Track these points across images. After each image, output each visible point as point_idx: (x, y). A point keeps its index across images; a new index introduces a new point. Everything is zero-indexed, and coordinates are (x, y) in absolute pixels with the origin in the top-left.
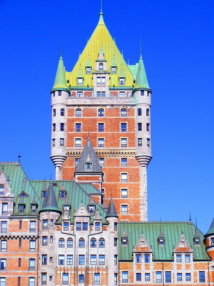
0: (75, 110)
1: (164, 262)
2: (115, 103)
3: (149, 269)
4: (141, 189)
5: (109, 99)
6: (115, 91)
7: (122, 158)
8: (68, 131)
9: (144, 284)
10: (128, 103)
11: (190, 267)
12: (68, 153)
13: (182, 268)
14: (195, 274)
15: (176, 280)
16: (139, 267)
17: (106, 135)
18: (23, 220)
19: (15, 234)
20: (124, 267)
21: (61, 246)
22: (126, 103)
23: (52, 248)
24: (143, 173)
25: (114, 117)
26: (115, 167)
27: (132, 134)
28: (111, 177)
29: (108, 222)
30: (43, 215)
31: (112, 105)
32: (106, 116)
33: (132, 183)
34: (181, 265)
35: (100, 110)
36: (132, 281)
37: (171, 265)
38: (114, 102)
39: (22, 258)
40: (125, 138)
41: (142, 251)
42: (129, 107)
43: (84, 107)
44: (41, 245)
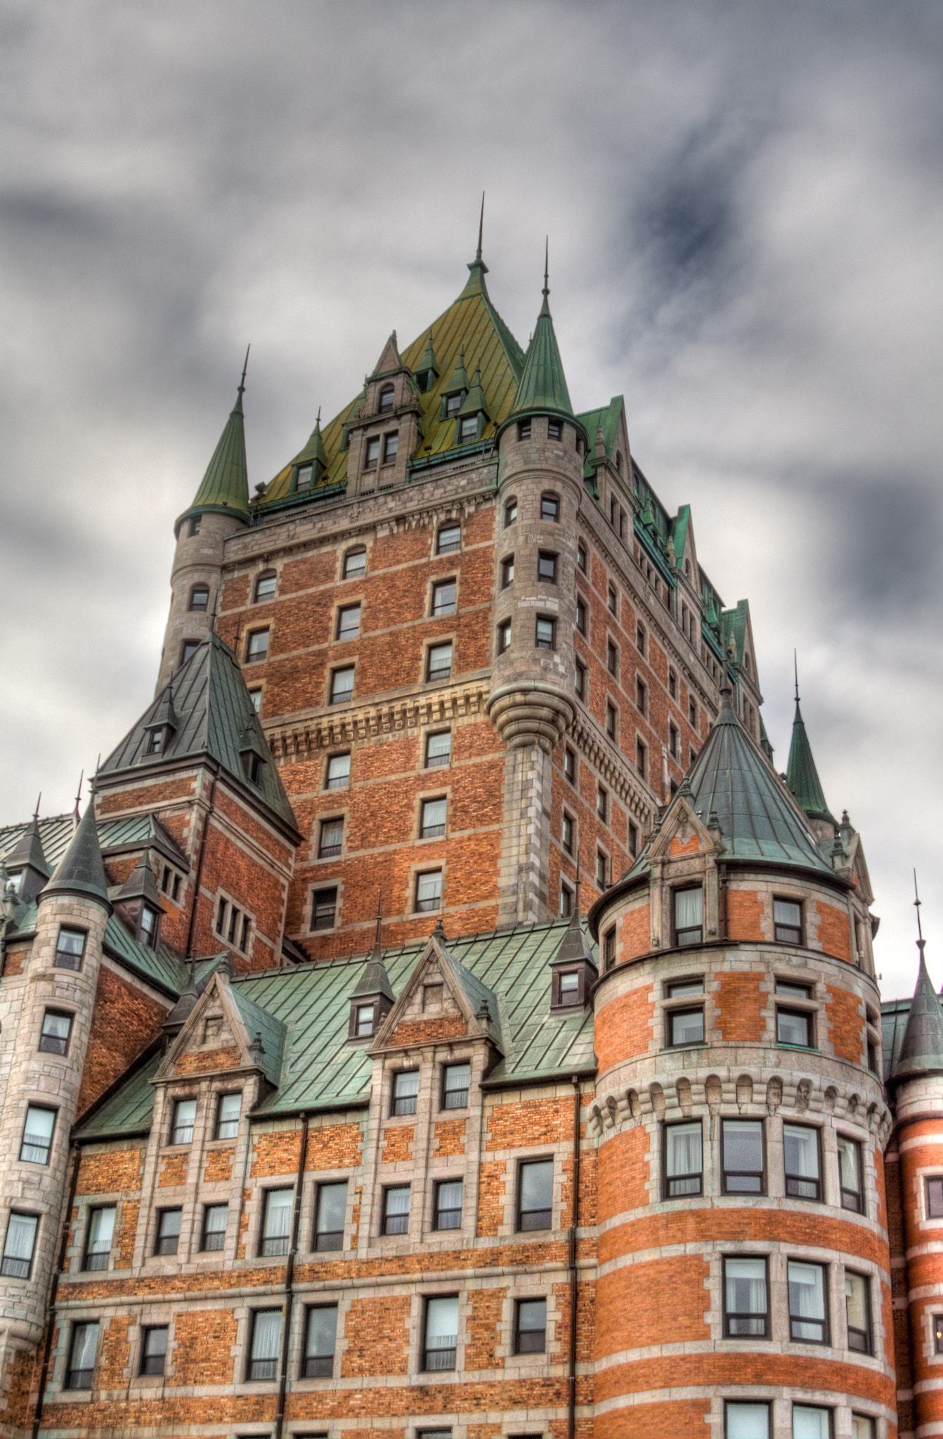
1: (314, 1123)
2: (412, 506)
3: (225, 1174)
4: (504, 854)
5: (389, 499)
6: (435, 471)
7: (424, 730)
9: (189, 1269)
10: (464, 491)
11: (464, 1139)
14: (487, 1178)
17: (362, 647)
20: (100, 1179)
22: (457, 493)
24: (519, 777)
25: (404, 566)
26: (393, 778)
27: (476, 613)
28: (371, 824)
31: (400, 520)
32: (374, 568)
33: (467, 833)
35: (349, 554)
36: (126, 1260)
37: (354, 1140)
38: (409, 505)
41: (205, 1068)
42: (470, 509)
43: (287, 560)
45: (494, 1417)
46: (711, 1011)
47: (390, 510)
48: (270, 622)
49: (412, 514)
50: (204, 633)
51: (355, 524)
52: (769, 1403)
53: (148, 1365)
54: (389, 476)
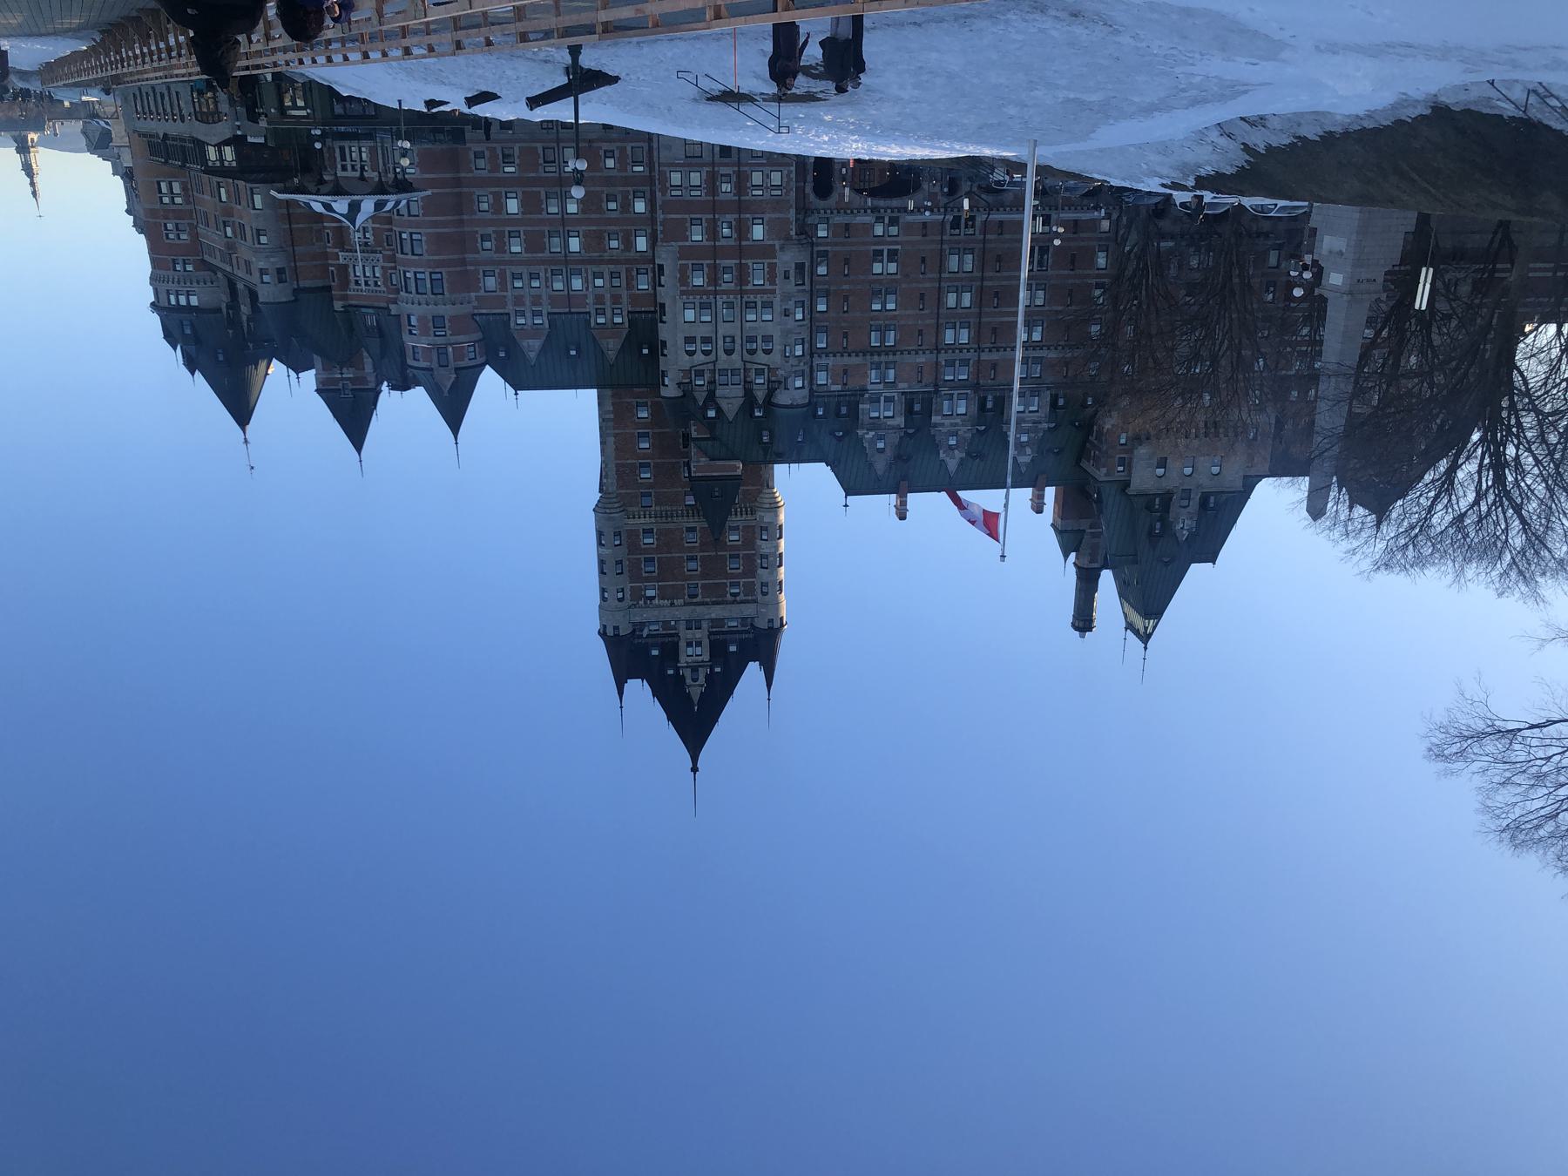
0: (742, 594)
1: (567, 310)
2: (667, 610)
7: (653, 508)
8: (754, 555)
12: (752, 514)
13: (532, 299)
15: (542, 275)
16: (616, 299)
18: (840, 386)
19: (854, 360)
21: (768, 339)
29: (679, 387)
30: (804, 397)
31: (672, 604)
33: (629, 462)
34: (534, 304)
35: (696, 596)
39: (841, 314)
40: (646, 546)
43: (725, 599)
44: (807, 339)
45: (495, 217)
46: (431, 324)
47: (677, 610)
48: (729, 571)
49: (667, 606)
50: (760, 571)
51: (693, 607)
52: (410, 215)
54: (689, 634)
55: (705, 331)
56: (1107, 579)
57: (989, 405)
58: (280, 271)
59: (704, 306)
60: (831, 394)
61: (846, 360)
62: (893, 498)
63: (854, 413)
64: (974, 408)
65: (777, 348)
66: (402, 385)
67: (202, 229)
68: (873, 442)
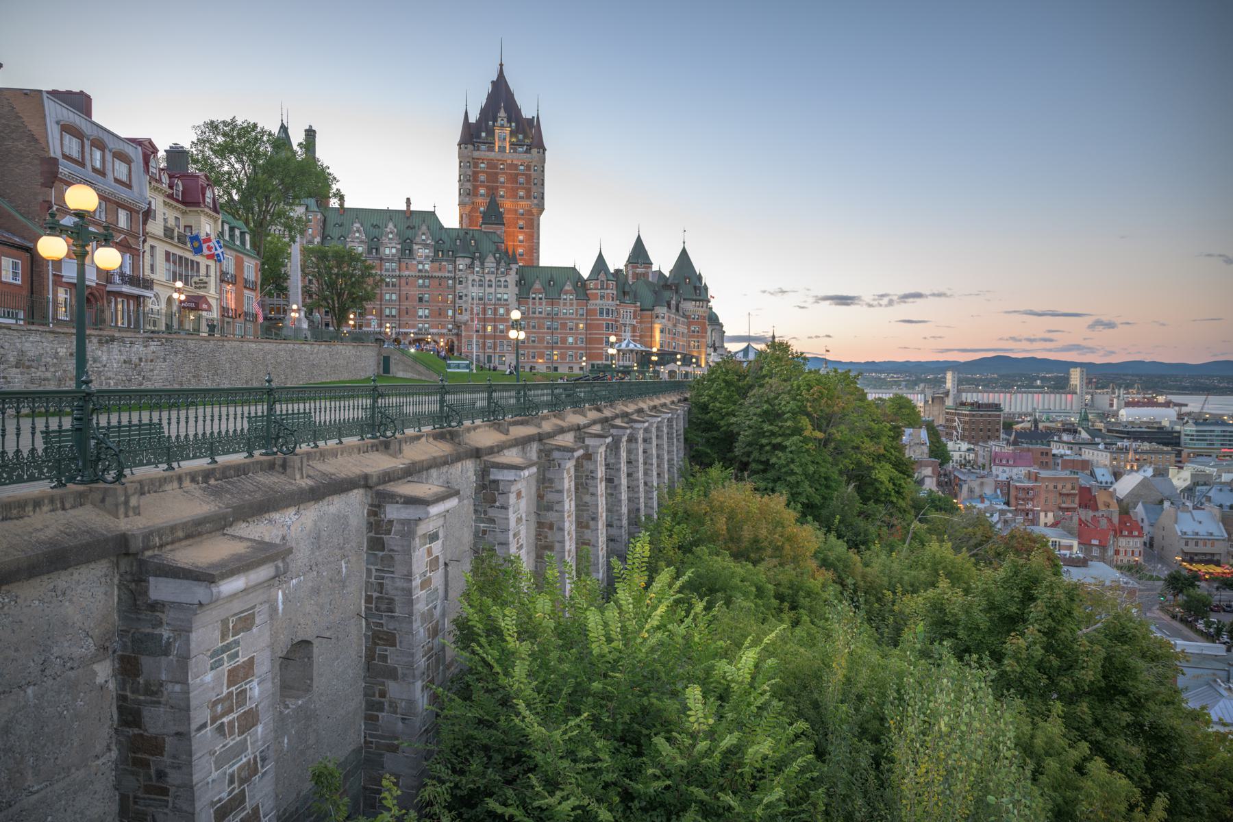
16: (534, 304)
19: (434, 274)
23: (466, 287)
53: (534, 327)
55: (499, 290)
56: (300, 153)
57: (374, 251)
58: (657, 317)
59: (499, 299)
60: (446, 261)
61: (440, 274)
62: (413, 208)
63: (436, 252)
64: (382, 249)
65: (470, 282)
66: (618, 271)
67: (686, 331)
68: (427, 238)
